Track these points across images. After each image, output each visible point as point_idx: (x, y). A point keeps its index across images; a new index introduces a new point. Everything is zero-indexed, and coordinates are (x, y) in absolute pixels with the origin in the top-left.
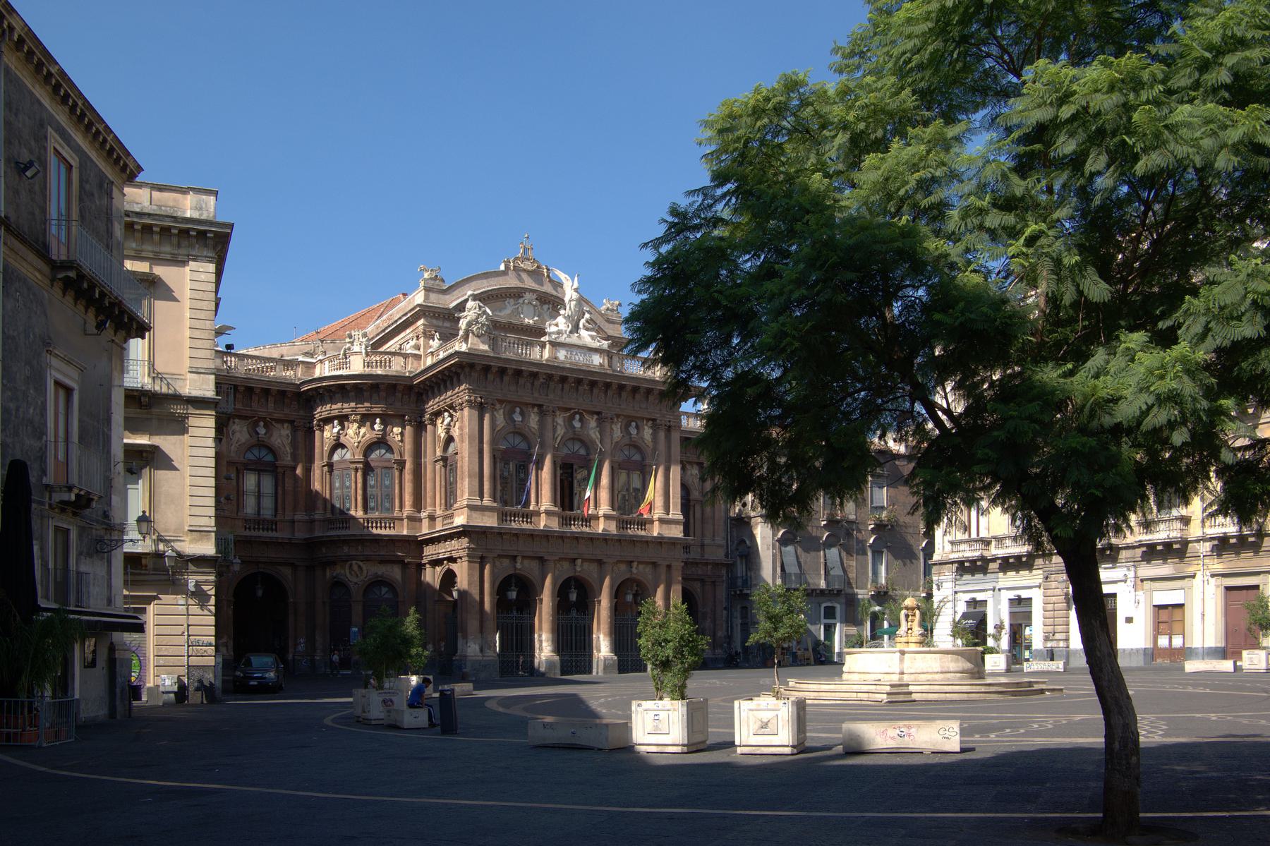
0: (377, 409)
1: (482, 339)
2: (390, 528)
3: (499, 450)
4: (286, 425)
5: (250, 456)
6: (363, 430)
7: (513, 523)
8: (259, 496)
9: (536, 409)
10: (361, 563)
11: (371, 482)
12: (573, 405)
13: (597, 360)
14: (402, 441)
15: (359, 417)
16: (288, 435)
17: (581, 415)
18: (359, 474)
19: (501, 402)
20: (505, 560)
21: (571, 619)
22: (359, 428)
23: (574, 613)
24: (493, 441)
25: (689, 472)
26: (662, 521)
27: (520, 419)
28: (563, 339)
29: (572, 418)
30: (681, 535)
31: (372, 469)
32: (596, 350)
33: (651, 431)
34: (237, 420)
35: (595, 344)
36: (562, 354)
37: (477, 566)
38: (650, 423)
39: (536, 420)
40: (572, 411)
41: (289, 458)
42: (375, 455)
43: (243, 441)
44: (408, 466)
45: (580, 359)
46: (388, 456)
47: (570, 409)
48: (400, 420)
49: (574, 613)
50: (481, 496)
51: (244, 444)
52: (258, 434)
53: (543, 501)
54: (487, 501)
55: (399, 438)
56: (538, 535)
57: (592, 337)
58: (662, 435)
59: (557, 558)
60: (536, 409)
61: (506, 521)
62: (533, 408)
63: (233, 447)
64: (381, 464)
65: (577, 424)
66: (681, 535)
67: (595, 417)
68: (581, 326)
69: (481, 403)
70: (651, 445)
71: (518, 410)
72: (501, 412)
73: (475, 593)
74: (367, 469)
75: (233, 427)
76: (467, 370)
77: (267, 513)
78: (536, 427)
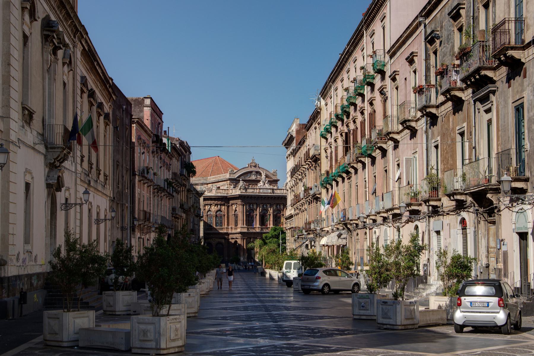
6: (215, 207)
24: (246, 212)
28: (262, 187)
29: (264, 205)
35: (269, 187)
42: (217, 213)
44: (226, 216)
45: (265, 191)
48: (224, 205)
54: (245, 226)
65: (265, 206)
73: (243, 245)
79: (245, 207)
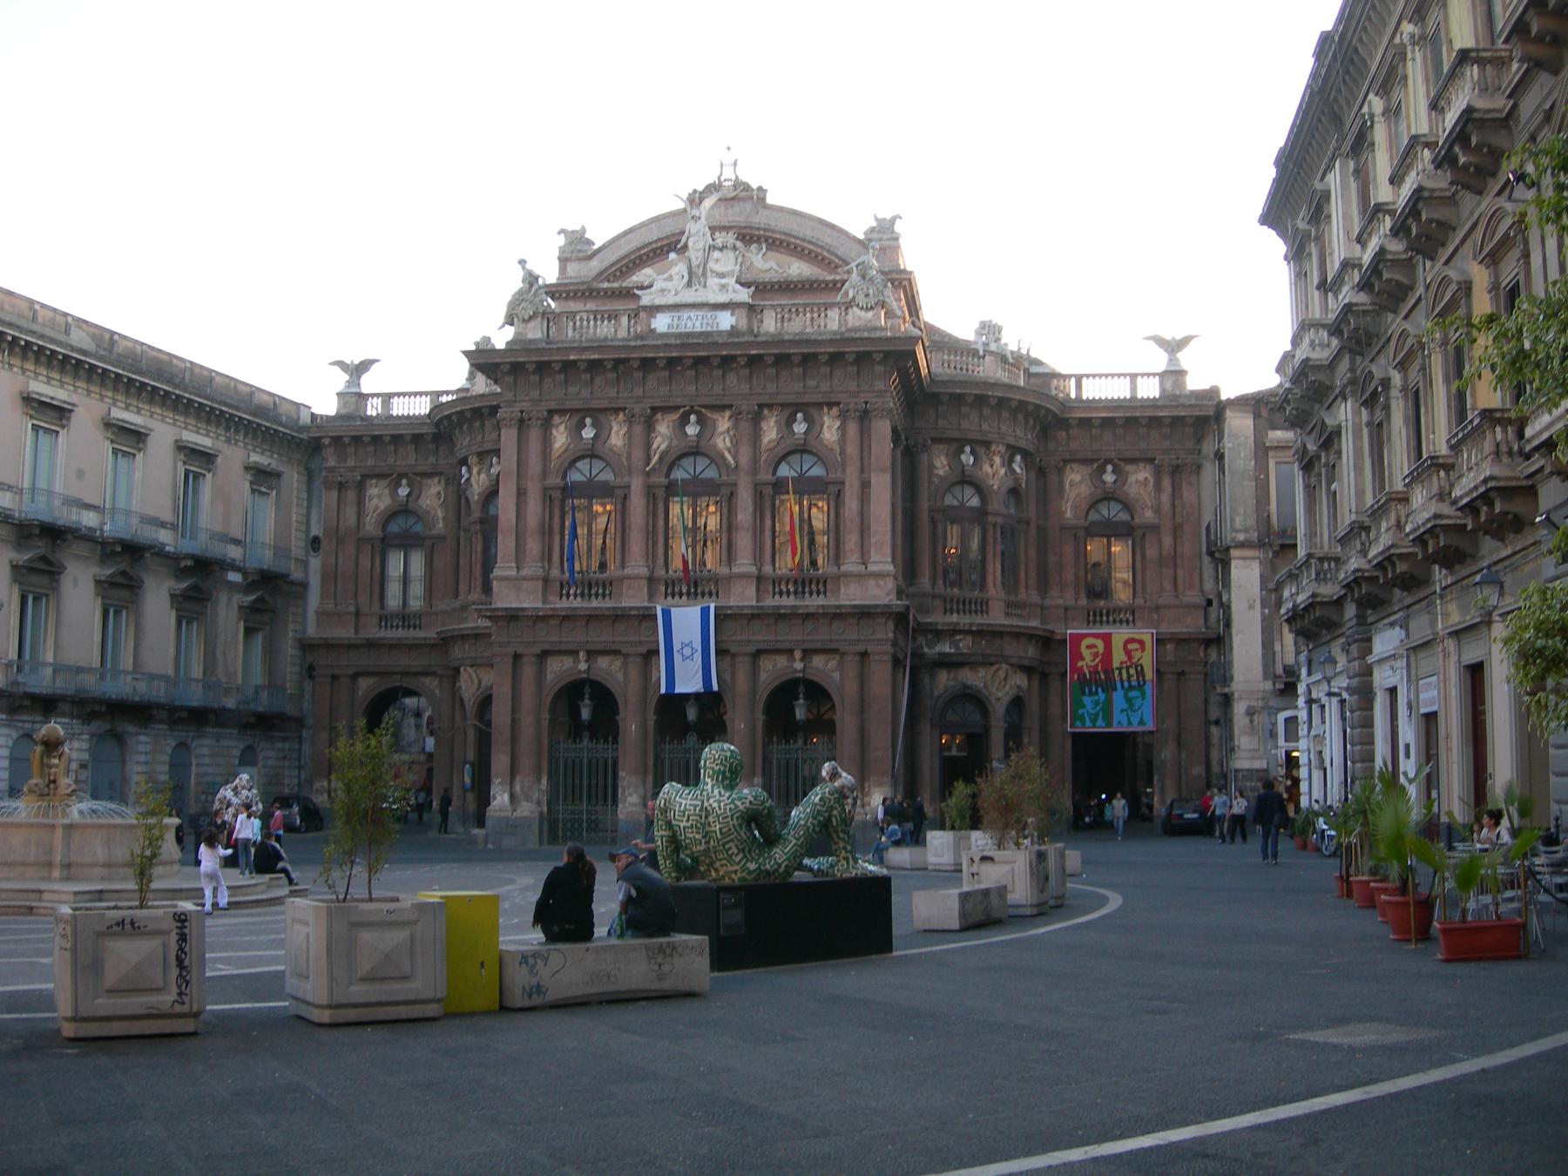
4: (436, 480)
5: (394, 528)
6: (483, 476)
8: (405, 579)
10: (469, 669)
12: (677, 401)
13: (726, 321)
16: (439, 493)
17: (698, 414)
21: (688, 751)
23: (692, 740)
25: (1132, 479)
29: (684, 420)
30: (886, 601)
34: (374, 481)
36: (661, 323)
38: (835, 411)
39: (622, 432)
41: (441, 525)
43: (382, 506)
45: (694, 323)
47: (677, 408)
58: (853, 429)
67: (727, 414)
70: (837, 448)
72: (562, 428)
77: (416, 604)
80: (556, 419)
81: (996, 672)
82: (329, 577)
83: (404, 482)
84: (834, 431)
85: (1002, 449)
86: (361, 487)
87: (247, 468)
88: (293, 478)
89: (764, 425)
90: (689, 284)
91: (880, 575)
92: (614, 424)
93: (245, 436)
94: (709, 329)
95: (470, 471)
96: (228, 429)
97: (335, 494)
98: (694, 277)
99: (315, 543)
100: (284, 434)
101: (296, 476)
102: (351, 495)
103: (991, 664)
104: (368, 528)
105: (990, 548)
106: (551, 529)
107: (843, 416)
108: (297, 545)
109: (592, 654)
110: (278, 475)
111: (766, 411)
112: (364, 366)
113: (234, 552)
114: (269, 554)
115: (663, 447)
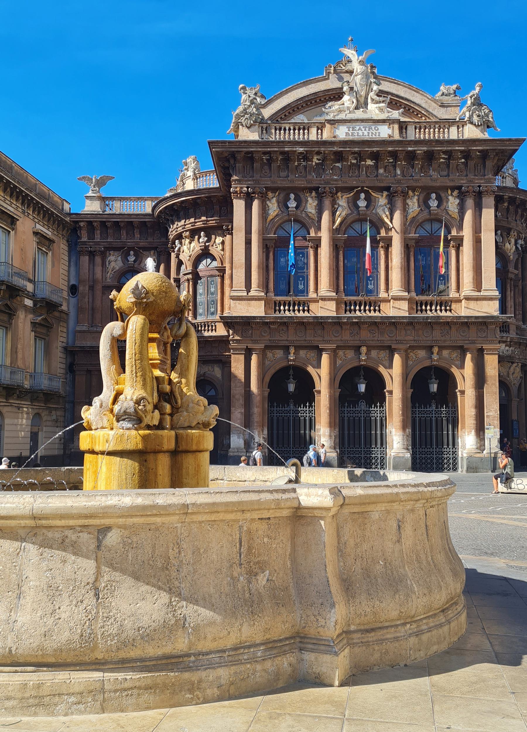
0: (199, 225)
1: (252, 129)
2: (212, 330)
3: (271, 239)
4: (152, 252)
6: (193, 244)
7: (287, 312)
9: (314, 194)
11: (200, 289)
14: (223, 250)
15: (188, 233)
17: (367, 193)
18: (191, 283)
19: (274, 190)
20: (278, 351)
22: (190, 243)
23: (363, 406)
24: (263, 231)
26: (468, 298)
27: (295, 205)
28: (342, 116)
29: (356, 198)
30: (496, 313)
31: (200, 278)
32: (384, 121)
33: (457, 201)
37: (242, 357)
38: (456, 193)
39: (315, 204)
40: (355, 191)
42: (202, 266)
43: (118, 268)
46: (215, 264)
49: (363, 406)
50: (248, 286)
51: (119, 270)
52: (128, 261)
53: (322, 287)
55: (220, 247)
56: (309, 323)
57: (381, 110)
59: (334, 346)
60: (314, 194)
61: (280, 311)
62: (311, 193)
63: (109, 274)
64: (208, 273)
65: (362, 204)
66: (496, 313)
67: (385, 193)
68: (369, 100)
69: (248, 194)
71: (292, 196)
74: (196, 277)
75: (109, 258)
76: (232, 162)
78: (313, 211)
79: (256, 204)
80: (270, 195)
81: (514, 369)
82: (79, 310)
83: (132, 253)
84: (456, 207)
85: (516, 234)
86: (104, 255)
87: (36, 233)
88: (62, 246)
89: (409, 201)
90: (357, 108)
91: (491, 299)
92: (309, 199)
93: (33, 211)
94: (374, 136)
95: (181, 243)
96: (23, 204)
97: (87, 257)
98: (361, 104)
99: (73, 290)
100: (57, 215)
101: (62, 246)
102: (98, 260)
103: (513, 363)
104: (108, 280)
105: (508, 293)
106: (267, 266)
107: (462, 196)
108: (63, 285)
109: (298, 348)
110: (51, 241)
111: (410, 193)
112: (101, 183)
113: (30, 287)
114: (48, 289)
115: (344, 214)
